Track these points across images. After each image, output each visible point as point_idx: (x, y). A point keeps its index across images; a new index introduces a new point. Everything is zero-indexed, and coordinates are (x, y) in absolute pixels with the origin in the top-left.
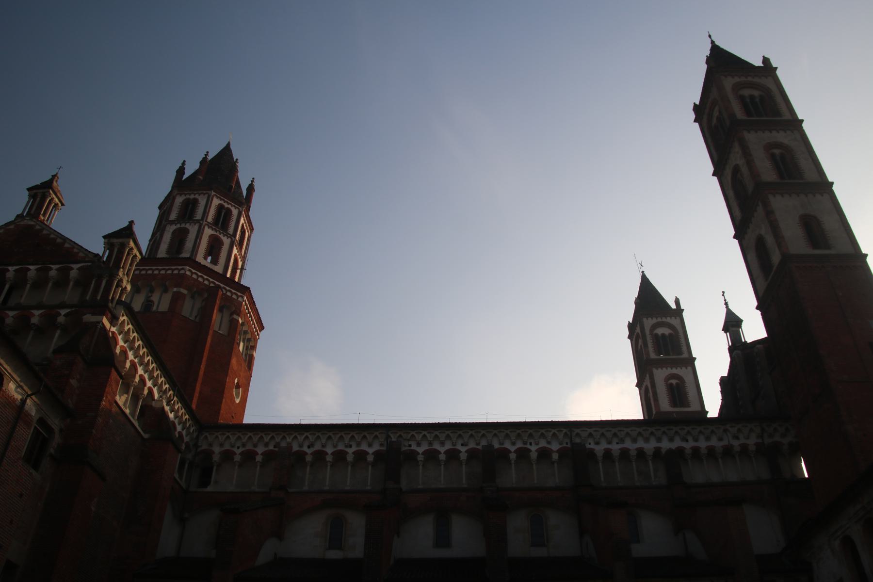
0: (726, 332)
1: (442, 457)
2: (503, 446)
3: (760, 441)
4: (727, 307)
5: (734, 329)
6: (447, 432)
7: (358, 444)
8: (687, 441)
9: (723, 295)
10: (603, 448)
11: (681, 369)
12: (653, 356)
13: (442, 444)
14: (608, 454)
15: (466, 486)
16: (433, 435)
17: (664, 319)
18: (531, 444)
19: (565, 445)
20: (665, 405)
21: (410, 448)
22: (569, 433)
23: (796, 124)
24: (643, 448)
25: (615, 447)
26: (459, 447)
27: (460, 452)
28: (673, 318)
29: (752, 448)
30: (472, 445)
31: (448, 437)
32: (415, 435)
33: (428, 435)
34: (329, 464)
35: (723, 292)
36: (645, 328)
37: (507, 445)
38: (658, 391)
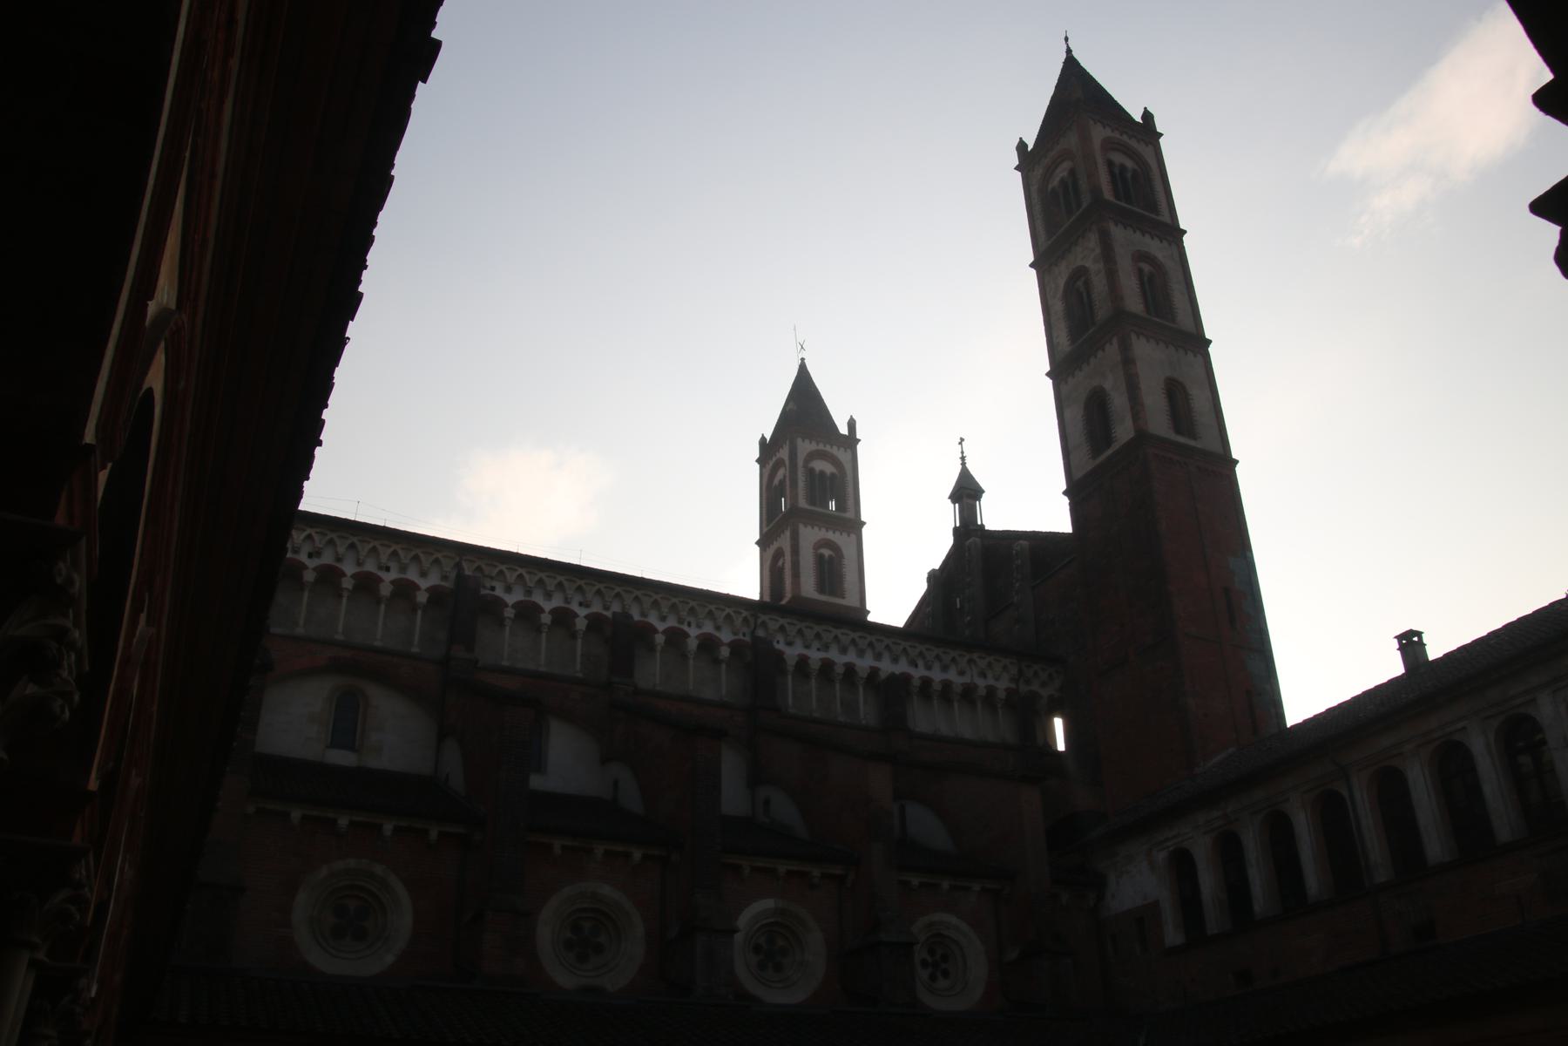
1: (546, 619)
2: (646, 620)
3: (1013, 686)
4: (963, 464)
5: (970, 501)
6: (560, 578)
7: (403, 569)
8: (916, 666)
9: (960, 443)
10: (797, 653)
11: (841, 534)
12: (802, 503)
13: (548, 596)
14: (803, 661)
15: (580, 675)
16: (536, 578)
17: (828, 448)
18: (689, 625)
19: (741, 637)
20: (809, 588)
21: (491, 592)
22: (752, 621)
23: (1174, 234)
24: (854, 665)
25: (815, 656)
26: (575, 607)
27: (576, 615)
28: (842, 449)
29: (1002, 694)
30: (596, 608)
31: (560, 586)
32: (506, 571)
33: (527, 577)
34: (345, 594)
35: (962, 440)
36: (799, 454)
37: (653, 619)
38: (802, 563)
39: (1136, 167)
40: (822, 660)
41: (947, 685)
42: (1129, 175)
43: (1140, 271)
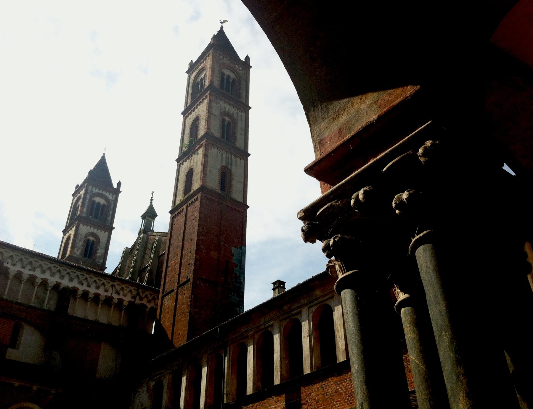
0: (143, 219)
3: (133, 300)
4: (151, 202)
8: (82, 284)
9: (152, 194)
10: (17, 270)
14: (18, 276)
17: (104, 193)
23: (246, 108)
24: (48, 280)
25: (27, 272)
29: (126, 304)
35: (153, 192)
39: (235, 77)
40: (30, 275)
41: (97, 296)
42: (231, 80)
43: (223, 121)
